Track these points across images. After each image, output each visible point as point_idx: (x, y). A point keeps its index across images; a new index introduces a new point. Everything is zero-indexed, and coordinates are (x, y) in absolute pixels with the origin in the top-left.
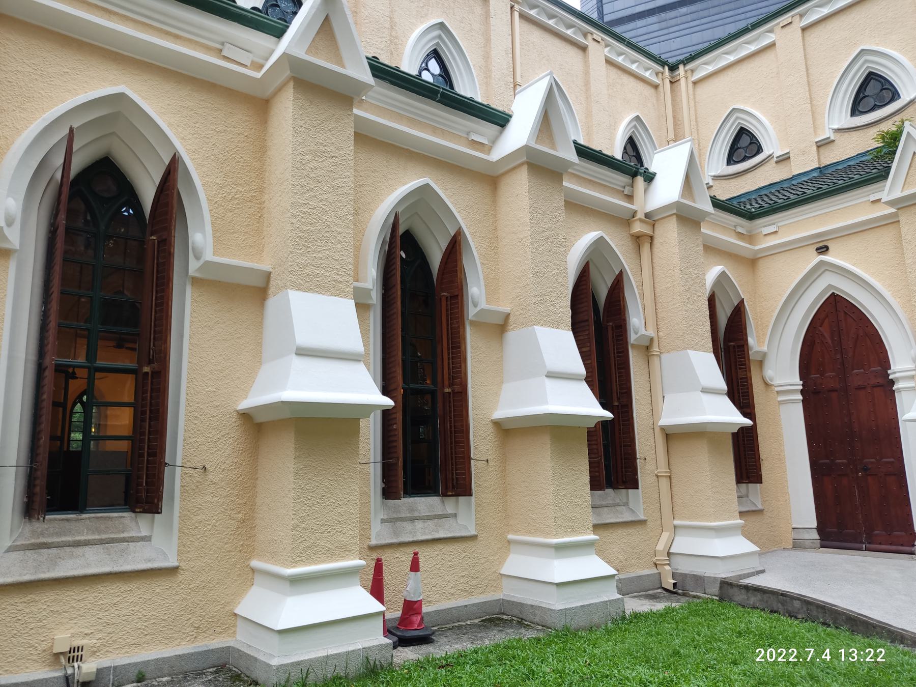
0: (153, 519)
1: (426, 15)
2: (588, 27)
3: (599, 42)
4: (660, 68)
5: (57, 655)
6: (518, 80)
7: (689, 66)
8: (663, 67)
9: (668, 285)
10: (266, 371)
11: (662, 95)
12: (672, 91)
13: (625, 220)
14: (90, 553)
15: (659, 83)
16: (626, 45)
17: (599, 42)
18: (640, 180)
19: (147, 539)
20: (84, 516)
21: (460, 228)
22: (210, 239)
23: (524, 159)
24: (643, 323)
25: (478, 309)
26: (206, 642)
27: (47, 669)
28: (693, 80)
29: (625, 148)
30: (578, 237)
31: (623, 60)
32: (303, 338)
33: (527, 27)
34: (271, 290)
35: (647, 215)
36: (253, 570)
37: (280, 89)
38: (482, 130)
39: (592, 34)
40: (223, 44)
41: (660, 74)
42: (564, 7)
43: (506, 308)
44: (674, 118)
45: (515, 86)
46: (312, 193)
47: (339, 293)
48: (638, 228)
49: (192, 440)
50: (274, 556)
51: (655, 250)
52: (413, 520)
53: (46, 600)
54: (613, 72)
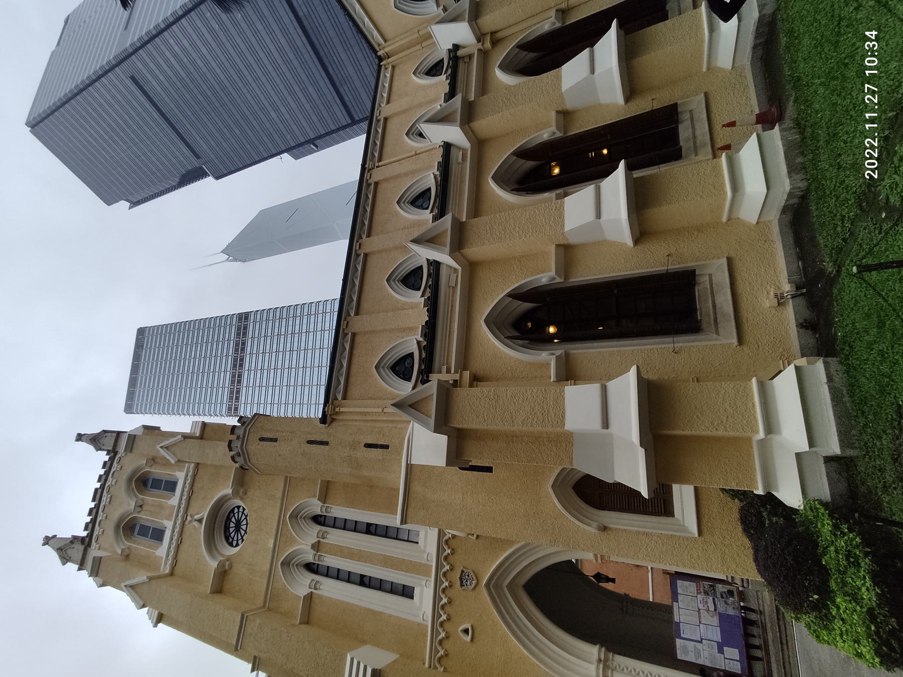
0: (699, 275)
1: (396, 212)
5: (779, 304)
6: (413, 153)
7: (377, 49)
8: (382, 66)
9: (520, 10)
10: (611, 236)
11: (398, 61)
12: (393, 56)
13: (484, 55)
14: (719, 300)
18: (460, 53)
19: (710, 276)
20: (698, 307)
21: (512, 154)
22: (545, 274)
23: (467, 126)
24: (547, 20)
25: (556, 131)
26: (775, 235)
27: (787, 308)
28: (383, 43)
29: (433, 76)
30: (501, 82)
31: (385, 93)
32: (590, 216)
33: (385, 156)
34: (565, 242)
35: (479, 41)
36: (729, 220)
37: (465, 257)
38: (457, 156)
40: (450, 287)
43: (553, 114)
44: (408, 49)
45: (417, 154)
46: (512, 231)
47: (562, 207)
48: (488, 45)
49: (653, 264)
50: (720, 207)
51: (498, 28)
52: (695, 137)
53: (747, 314)
54: (393, 97)
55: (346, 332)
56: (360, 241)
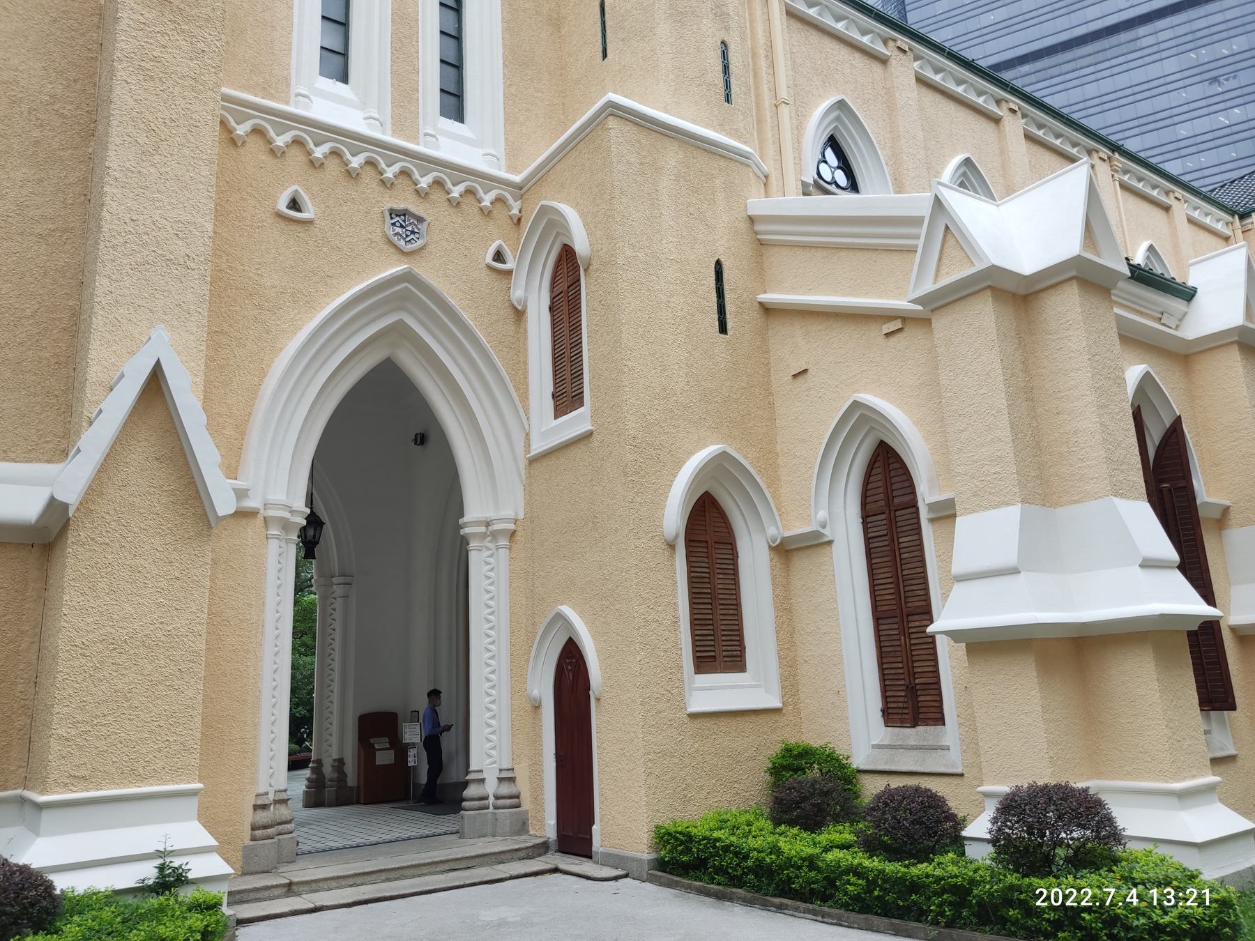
2: (945, 61)
3: (904, 51)
4: (1229, 218)
8: (1233, 216)
15: (1002, 114)
16: (1009, 92)
17: (1179, 200)
39: (1007, 102)
41: (1230, 224)
42: (882, 19)
55: (891, 43)
56: (1019, 114)
